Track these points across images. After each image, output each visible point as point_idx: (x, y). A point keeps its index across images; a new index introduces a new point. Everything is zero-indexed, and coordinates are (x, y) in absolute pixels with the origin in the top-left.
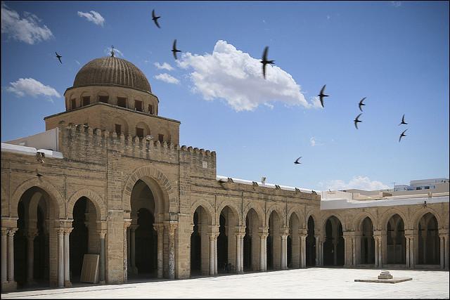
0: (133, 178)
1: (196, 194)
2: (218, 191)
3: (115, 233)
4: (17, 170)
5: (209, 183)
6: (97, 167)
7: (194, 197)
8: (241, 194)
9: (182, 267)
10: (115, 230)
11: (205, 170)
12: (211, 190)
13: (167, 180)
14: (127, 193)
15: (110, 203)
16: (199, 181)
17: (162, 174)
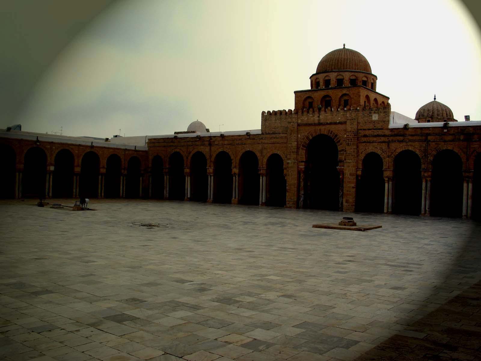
0: (308, 138)
1: (364, 144)
2: (391, 138)
3: (291, 176)
4: (238, 144)
5: (380, 132)
6: (282, 135)
7: (362, 147)
8: (424, 138)
9: (347, 201)
10: (291, 174)
11: (374, 122)
12: (383, 139)
13: (336, 136)
14: (302, 149)
15: (288, 157)
16: (367, 133)
17: (332, 131)
